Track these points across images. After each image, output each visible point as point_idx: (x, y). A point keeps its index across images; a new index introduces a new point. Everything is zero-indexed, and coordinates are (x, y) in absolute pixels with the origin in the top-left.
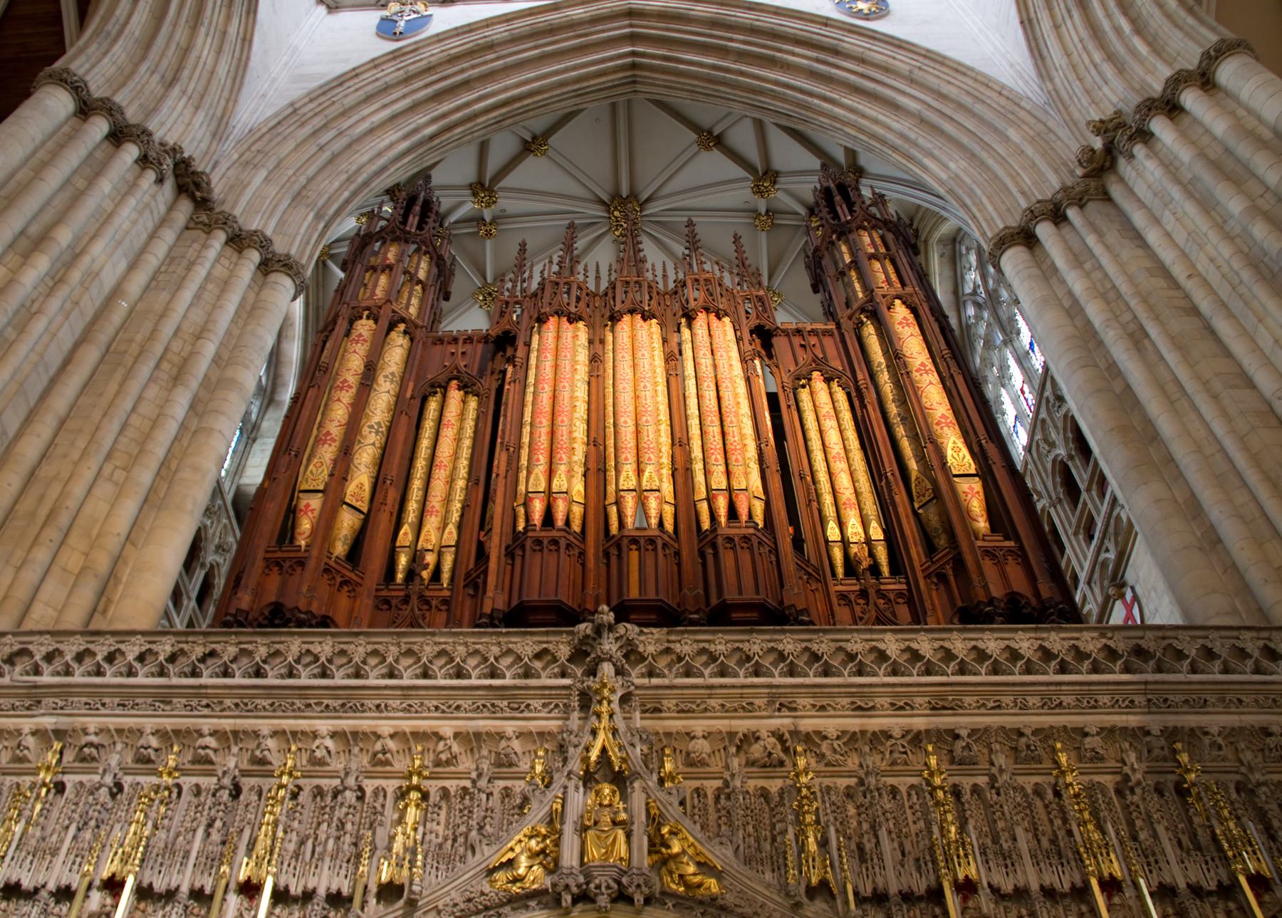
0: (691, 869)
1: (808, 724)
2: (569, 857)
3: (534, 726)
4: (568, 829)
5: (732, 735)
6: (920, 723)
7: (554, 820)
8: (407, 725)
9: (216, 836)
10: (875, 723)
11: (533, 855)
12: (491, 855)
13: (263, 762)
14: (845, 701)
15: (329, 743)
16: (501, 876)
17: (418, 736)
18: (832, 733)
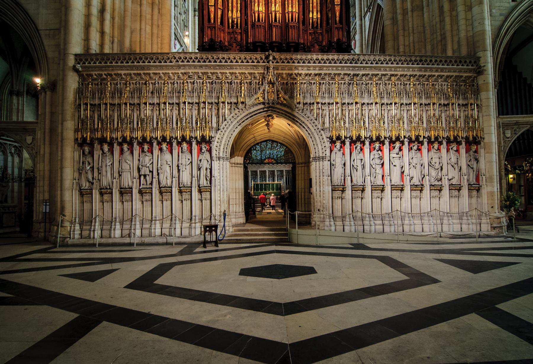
0: (282, 99)
1: (300, 72)
2: (266, 98)
3: (260, 72)
4: (266, 93)
5: (289, 74)
6: (317, 72)
7: (264, 91)
8: (241, 71)
9: (216, 93)
10: (310, 72)
11: (261, 97)
12: (255, 97)
13: (219, 78)
14: (306, 68)
15: (229, 74)
16: (257, 100)
17: (242, 73)
18: (303, 74)
